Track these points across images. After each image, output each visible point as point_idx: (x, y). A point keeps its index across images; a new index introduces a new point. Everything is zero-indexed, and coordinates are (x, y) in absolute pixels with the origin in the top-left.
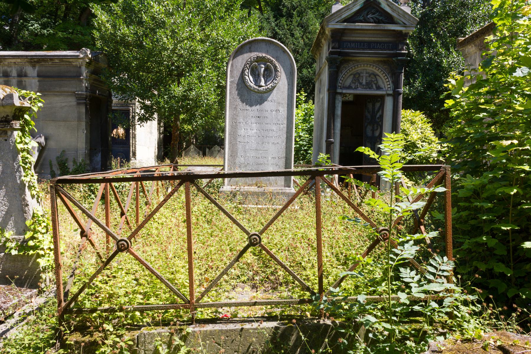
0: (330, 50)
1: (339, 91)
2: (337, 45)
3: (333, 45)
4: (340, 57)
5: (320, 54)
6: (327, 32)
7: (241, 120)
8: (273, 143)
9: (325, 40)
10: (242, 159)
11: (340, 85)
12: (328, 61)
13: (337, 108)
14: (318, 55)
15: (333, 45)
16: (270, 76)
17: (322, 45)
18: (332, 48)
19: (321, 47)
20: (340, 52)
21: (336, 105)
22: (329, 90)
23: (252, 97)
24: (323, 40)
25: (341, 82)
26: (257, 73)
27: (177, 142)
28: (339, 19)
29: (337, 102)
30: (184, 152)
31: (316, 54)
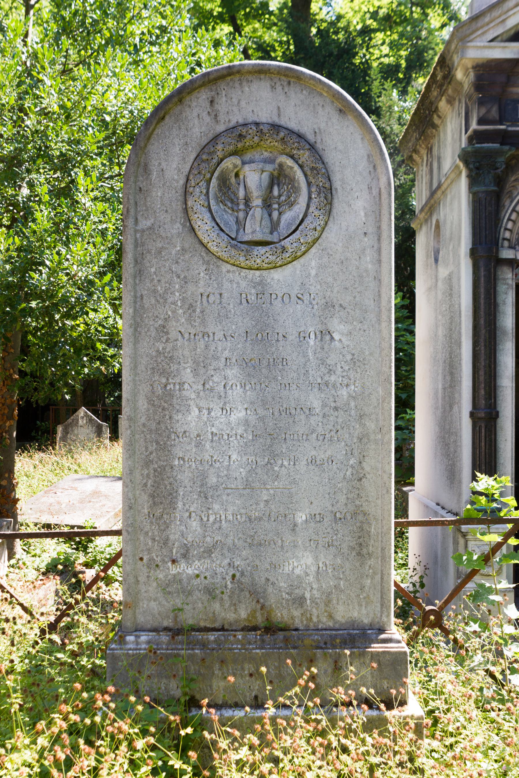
0: (474, 126)
1: (507, 254)
2: (494, 113)
3: (483, 111)
4: (506, 148)
5: (430, 150)
6: (459, 75)
7: (187, 375)
8: (313, 461)
9: (450, 102)
10: (195, 524)
11: (507, 235)
12: (466, 163)
13: (501, 308)
14: (423, 152)
15: (483, 111)
16: (291, 205)
17: (436, 120)
18: (480, 122)
19: (434, 126)
20: (505, 131)
21: (500, 298)
22: (473, 253)
23: (226, 285)
24: (443, 104)
25: (510, 225)
26: (241, 193)
27: (14, 423)
28: (499, 31)
29: (501, 288)
30: (60, 429)
31: (415, 151)
